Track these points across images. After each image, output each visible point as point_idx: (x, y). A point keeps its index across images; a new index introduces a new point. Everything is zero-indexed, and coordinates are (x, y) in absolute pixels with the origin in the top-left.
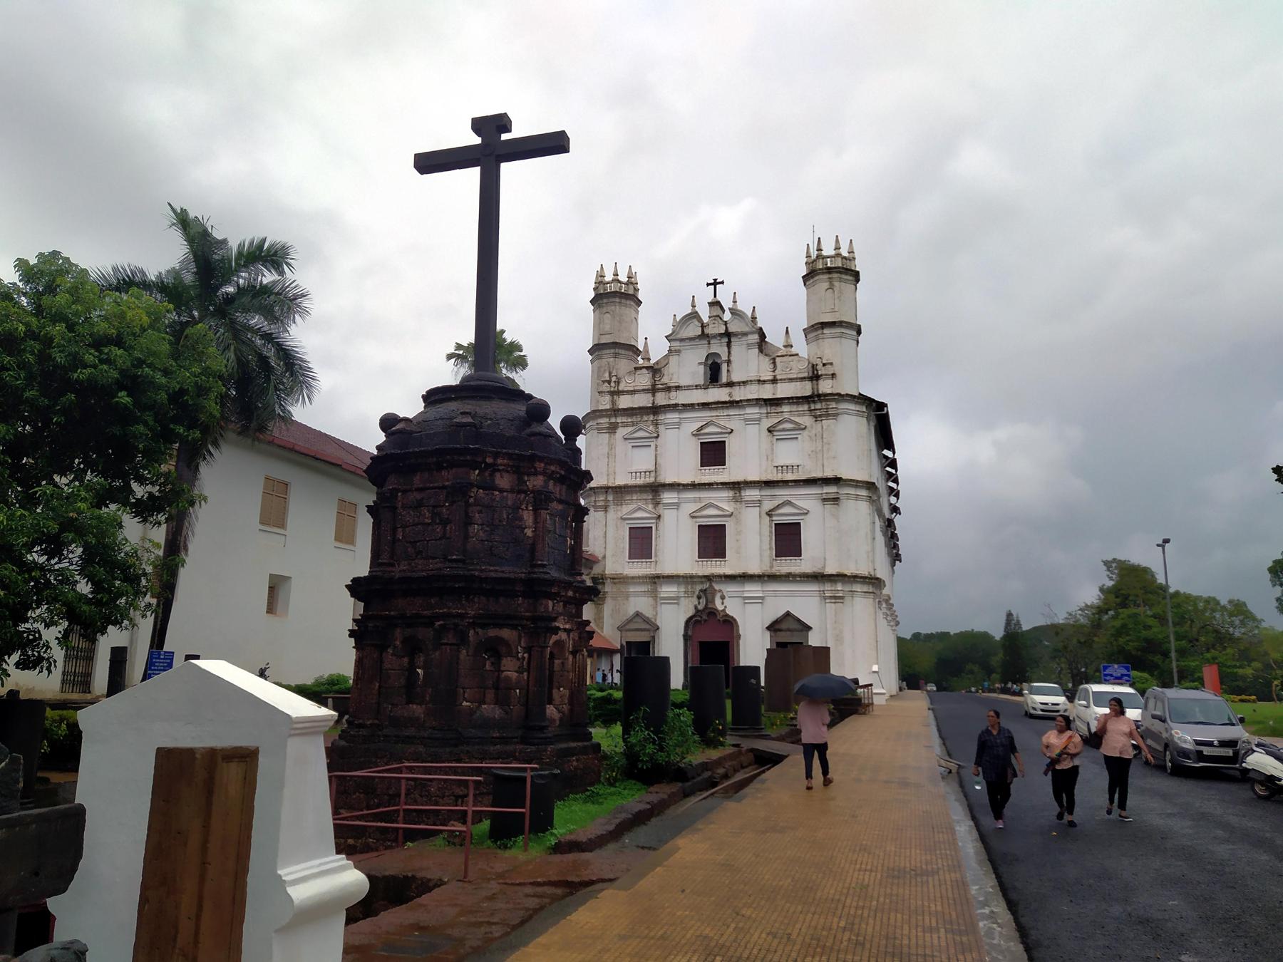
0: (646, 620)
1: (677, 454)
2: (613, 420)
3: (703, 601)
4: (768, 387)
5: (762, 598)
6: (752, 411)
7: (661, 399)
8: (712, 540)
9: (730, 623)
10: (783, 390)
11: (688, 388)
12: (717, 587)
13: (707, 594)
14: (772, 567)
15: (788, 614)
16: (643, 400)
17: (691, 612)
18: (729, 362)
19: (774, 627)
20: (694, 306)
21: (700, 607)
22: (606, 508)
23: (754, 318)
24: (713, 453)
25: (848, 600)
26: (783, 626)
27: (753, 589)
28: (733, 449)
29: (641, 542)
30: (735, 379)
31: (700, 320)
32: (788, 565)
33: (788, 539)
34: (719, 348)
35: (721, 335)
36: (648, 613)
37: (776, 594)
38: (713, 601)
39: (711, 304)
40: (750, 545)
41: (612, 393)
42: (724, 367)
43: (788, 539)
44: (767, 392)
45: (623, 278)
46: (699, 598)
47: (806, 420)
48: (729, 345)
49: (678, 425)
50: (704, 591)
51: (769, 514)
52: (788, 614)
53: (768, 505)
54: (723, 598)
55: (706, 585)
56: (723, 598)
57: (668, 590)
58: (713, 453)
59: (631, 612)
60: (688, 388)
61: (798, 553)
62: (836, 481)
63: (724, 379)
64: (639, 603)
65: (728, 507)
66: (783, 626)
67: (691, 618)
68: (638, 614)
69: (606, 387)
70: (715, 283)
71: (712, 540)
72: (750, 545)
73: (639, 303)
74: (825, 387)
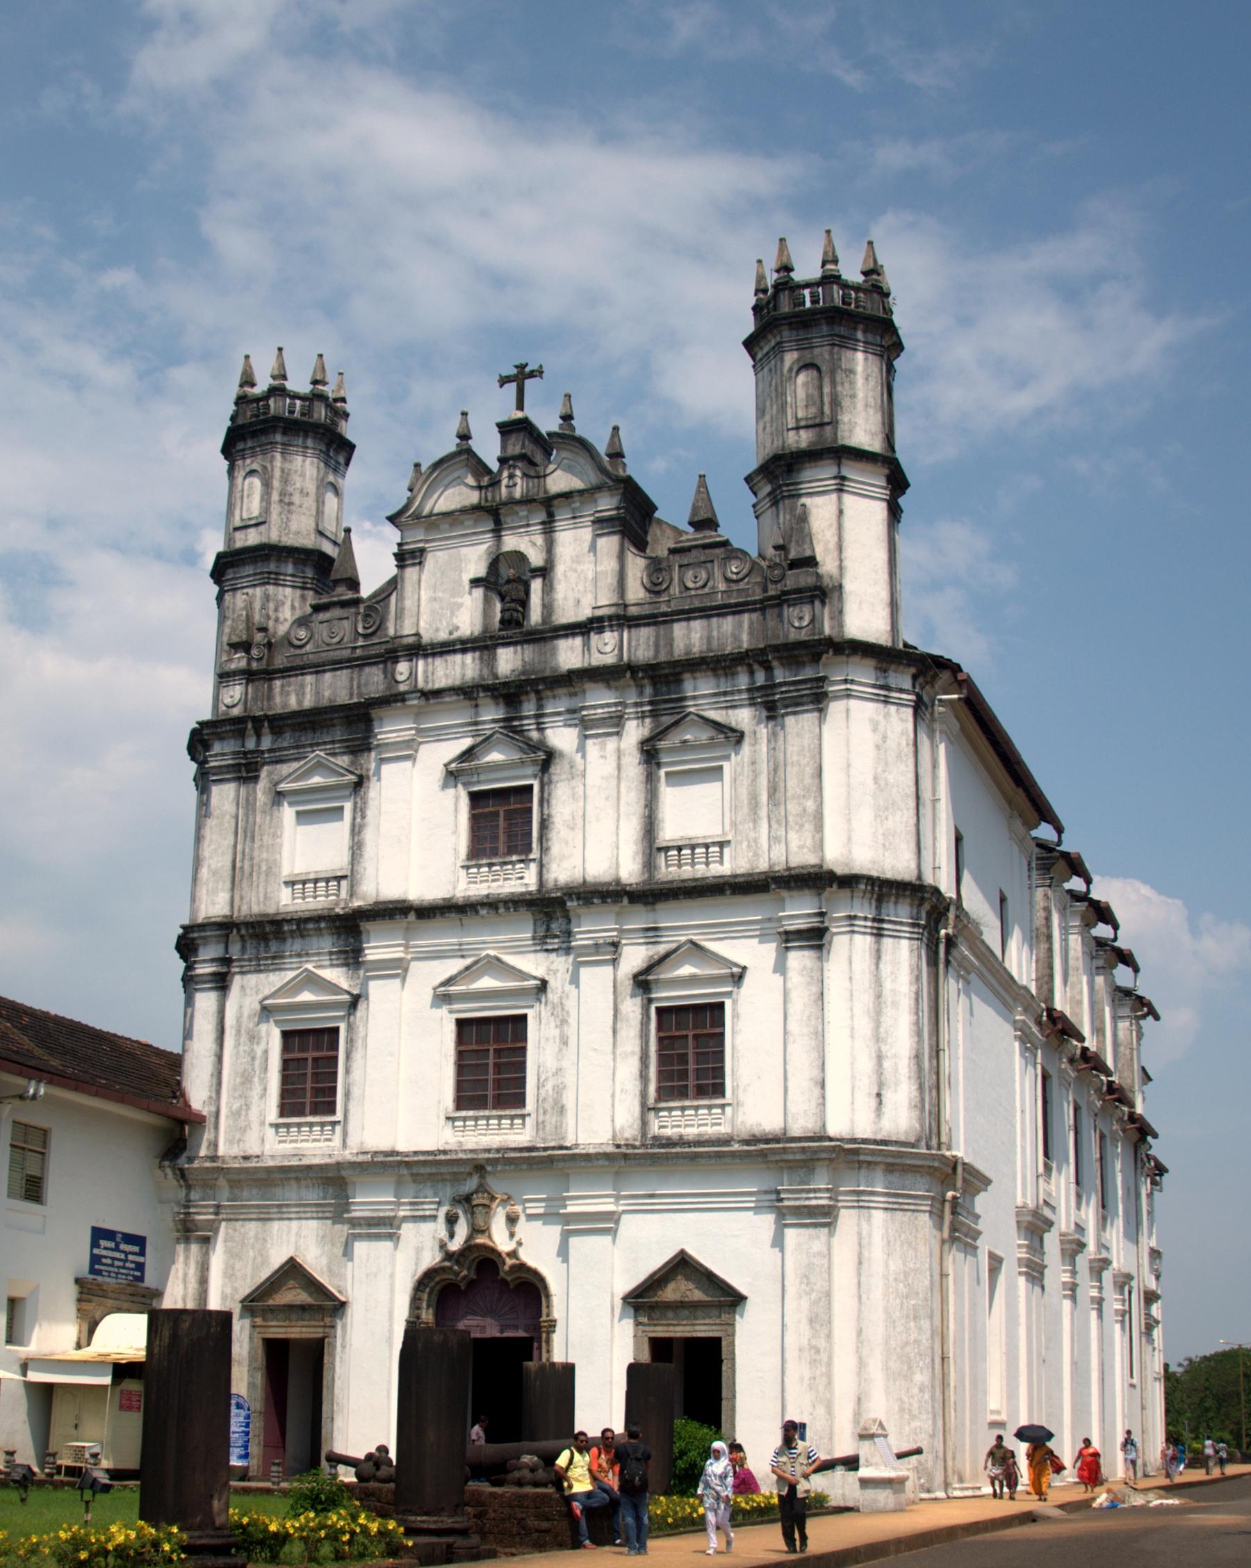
1: (411, 827)
2: (251, 744)
3: (462, 1230)
4: (645, 634)
5: (613, 1217)
6: (600, 699)
7: (374, 681)
8: (491, 1059)
9: (528, 1290)
10: (690, 637)
14: (644, 1123)
15: (682, 1264)
16: (334, 688)
17: (431, 1258)
18: (545, 572)
19: (642, 1301)
20: (464, 436)
21: (455, 1245)
22: (221, 983)
23: (617, 455)
25: (847, 1219)
26: (670, 1293)
29: (312, 1071)
30: (567, 614)
31: (479, 467)
32: (688, 1122)
33: (688, 1048)
34: (524, 542)
35: (527, 501)
36: (315, 1261)
37: (649, 1205)
38: (485, 1231)
39: (507, 429)
40: (590, 1072)
41: (249, 676)
42: (536, 585)
43: (688, 1048)
44: (641, 645)
45: (299, 383)
46: (451, 1221)
47: (743, 717)
48: (548, 528)
49: (407, 751)
50: (467, 1199)
51: (643, 982)
52: (682, 1264)
53: (635, 957)
54: (512, 1220)
55: (471, 1184)
56: (512, 1220)
58: (503, 820)
59: (277, 1259)
61: (718, 1090)
62: (817, 880)
63: (535, 615)
65: (533, 964)
66: (670, 1293)
67: (429, 1275)
68: (292, 1270)
69: (239, 661)
70: (521, 377)
71: (491, 1059)
72: (590, 1072)
73: (347, 448)
74: (797, 622)
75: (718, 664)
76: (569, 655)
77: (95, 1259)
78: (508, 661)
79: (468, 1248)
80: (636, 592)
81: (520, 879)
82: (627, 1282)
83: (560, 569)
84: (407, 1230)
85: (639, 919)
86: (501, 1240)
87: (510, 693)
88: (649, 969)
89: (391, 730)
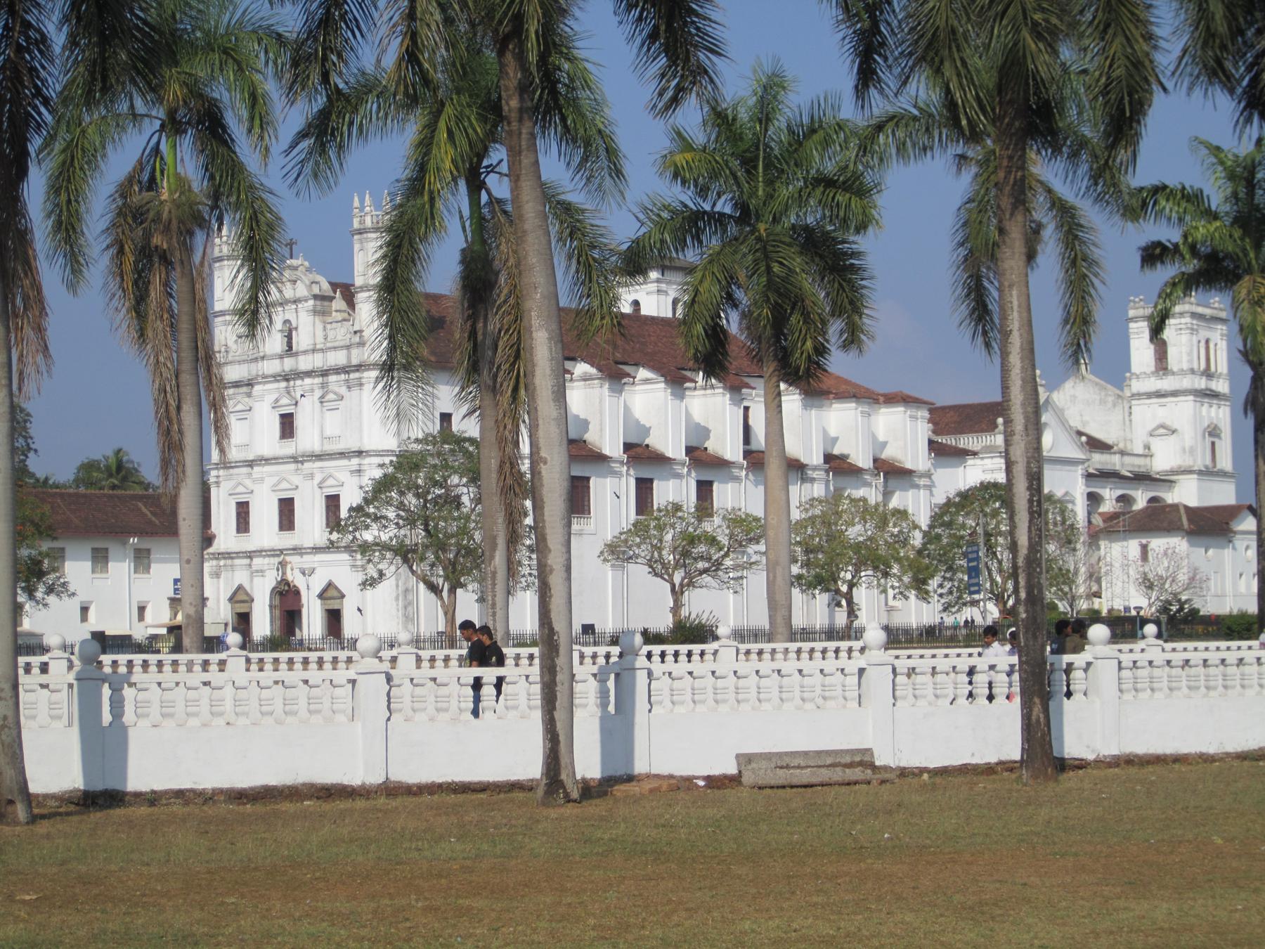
0: (247, 594)
9: (297, 593)
11: (272, 357)
12: (288, 559)
13: (283, 564)
17: (274, 584)
18: (296, 329)
24: (287, 425)
27: (308, 561)
28: (299, 422)
57: (257, 562)
58: (287, 425)
60: (272, 357)
62: (360, 453)
64: (240, 577)
65: (296, 480)
67: (274, 589)
68: (240, 588)
75: (338, 370)
76: (305, 363)
77: (176, 590)
78: (289, 364)
79: (282, 580)
80: (320, 339)
81: (288, 448)
82: (318, 591)
83: (300, 329)
84: (267, 573)
85: (319, 464)
86: (290, 578)
87: (286, 377)
88: (321, 483)
89: (257, 389)
